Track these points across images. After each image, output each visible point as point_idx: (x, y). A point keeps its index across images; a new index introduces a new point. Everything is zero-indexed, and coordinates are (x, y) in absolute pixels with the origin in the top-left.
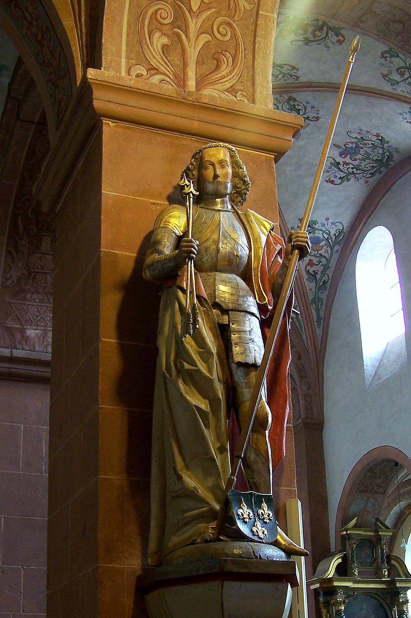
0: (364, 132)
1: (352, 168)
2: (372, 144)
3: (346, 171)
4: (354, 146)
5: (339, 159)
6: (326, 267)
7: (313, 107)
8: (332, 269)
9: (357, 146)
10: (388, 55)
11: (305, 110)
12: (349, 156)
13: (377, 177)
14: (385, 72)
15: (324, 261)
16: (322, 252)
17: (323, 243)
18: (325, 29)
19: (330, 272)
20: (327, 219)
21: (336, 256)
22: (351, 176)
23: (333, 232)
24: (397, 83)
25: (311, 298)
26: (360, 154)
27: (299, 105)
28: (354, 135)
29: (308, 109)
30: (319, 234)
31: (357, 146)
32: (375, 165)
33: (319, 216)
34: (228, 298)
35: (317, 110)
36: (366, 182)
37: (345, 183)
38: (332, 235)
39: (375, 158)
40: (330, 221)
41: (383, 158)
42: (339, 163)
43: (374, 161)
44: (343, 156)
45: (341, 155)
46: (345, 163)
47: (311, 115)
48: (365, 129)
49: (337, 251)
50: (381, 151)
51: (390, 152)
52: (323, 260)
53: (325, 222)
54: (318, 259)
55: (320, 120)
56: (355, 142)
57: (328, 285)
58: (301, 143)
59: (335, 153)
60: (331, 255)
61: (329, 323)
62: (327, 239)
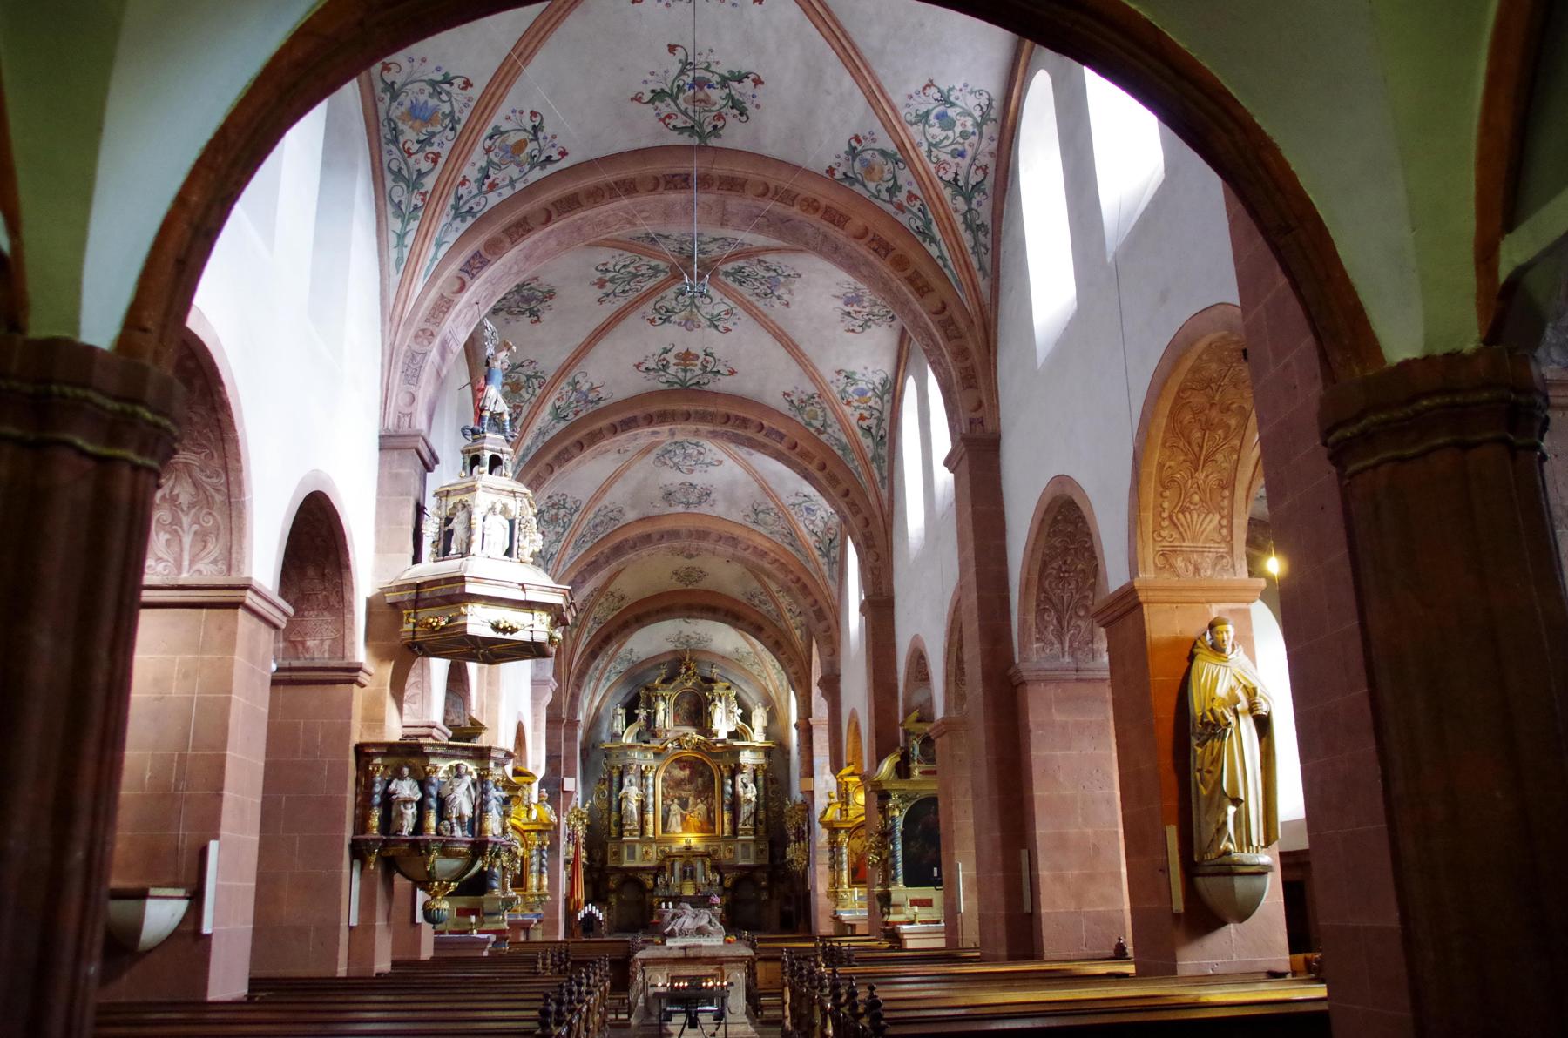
5: (848, 309)
6: (880, 420)
8: (888, 420)
15: (876, 414)
16: (871, 403)
17: (870, 394)
19: (886, 425)
20: (866, 368)
21: (888, 407)
23: (877, 380)
25: (870, 455)
29: (784, 268)
30: (862, 385)
33: (855, 366)
36: (890, 326)
37: (867, 330)
38: (877, 384)
40: (870, 370)
42: (849, 313)
45: (846, 304)
46: (856, 312)
49: (888, 401)
52: (875, 412)
53: (865, 372)
54: (868, 412)
55: (803, 276)
57: (886, 439)
58: (798, 298)
59: (840, 304)
60: (883, 408)
61: (892, 483)
62: (873, 390)
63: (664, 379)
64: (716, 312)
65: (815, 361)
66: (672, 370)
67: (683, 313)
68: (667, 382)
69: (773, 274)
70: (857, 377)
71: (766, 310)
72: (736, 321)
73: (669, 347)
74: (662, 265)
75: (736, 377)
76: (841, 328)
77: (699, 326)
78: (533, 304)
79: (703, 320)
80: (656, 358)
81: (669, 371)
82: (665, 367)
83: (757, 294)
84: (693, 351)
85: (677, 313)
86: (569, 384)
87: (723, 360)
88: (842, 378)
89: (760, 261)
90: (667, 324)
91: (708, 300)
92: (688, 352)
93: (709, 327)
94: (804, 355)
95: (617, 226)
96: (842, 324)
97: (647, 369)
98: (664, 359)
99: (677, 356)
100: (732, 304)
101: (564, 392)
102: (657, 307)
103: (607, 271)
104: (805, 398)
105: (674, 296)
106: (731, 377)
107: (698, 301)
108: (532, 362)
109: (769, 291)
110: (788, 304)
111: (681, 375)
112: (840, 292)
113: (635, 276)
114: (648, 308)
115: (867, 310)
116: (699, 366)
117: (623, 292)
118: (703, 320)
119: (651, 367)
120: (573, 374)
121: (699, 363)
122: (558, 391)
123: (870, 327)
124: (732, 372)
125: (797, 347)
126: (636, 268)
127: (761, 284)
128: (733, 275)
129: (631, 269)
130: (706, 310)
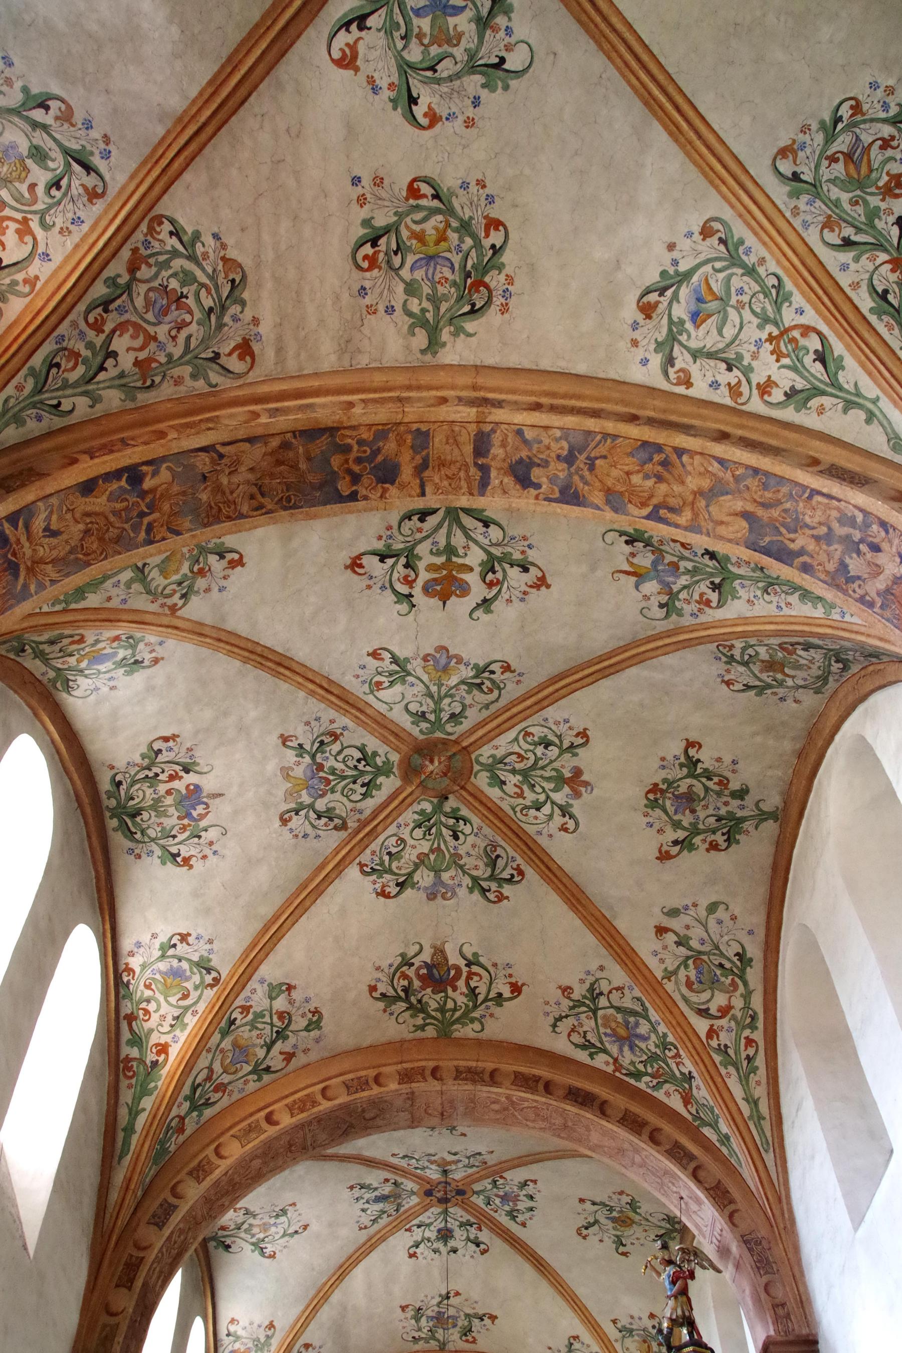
0: (208, 851)
1: (157, 775)
2: (174, 837)
3: (162, 766)
4: (195, 814)
5: (191, 778)
7: (305, 836)
9: (188, 815)
10: (315, 1019)
11: (311, 823)
12: (184, 792)
13: (105, 785)
14: (294, 994)
18: (402, 994)
22: (146, 762)
24: (272, 998)
26: (170, 806)
27: (326, 825)
28: (212, 834)
29: (309, 830)
31: (188, 815)
32: (131, 803)
34: (172, 435)
35: (297, 836)
36: (112, 767)
37: (144, 749)
39: (145, 815)
40: (105, 689)
41: (135, 824)
43: (142, 809)
44: (192, 787)
47: (296, 822)
48: (212, 859)
50: (152, 833)
51: (138, 841)
55: (278, 823)
56: (200, 820)
58: (272, 766)
59: (208, 784)
63: (495, 533)
64: (398, 688)
65: (205, 652)
66: (475, 557)
67: (454, 680)
68: (486, 525)
69: (321, 805)
70: (122, 671)
71: (315, 707)
72: (361, 672)
73: (479, 613)
74: (482, 780)
75: (345, 557)
76: (186, 730)
77: (425, 659)
78: (683, 789)
79: (420, 672)
80: (505, 595)
81: (480, 556)
82: (489, 567)
83: (336, 737)
84: (435, 602)
85: (463, 682)
86: (680, 613)
87: (376, 589)
88: (148, 657)
89: (344, 826)
90: (482, 664)
91: (413, 707)
92: (444, 598)
93: (407, 660)
94: (230, 653)
95: (526, 1104)
96: (188, 745)
97: (526, 570)
98: (491, 585)
99: (464, 590)
100: (370, 699)
101: (694, 607)
102: (496, 692)
103: (565, 811)
104: (201, 583)
105: (468, 713)
106: (354, 555)
107: (428, 705)
108: (728, 683)
109: (319, 758)
110: (284, 740)
111: (458, 539)
112: (220, 811)
113: (525, 774)
114: (512, 691)
115: (162, 788)
116: (421, 565)
117: (547, 744)
118: (420, 672)
119: (516, 569)
120: (662, 626)
121: (424, 576)
122: (703, 619)
123: (143, 756)
124: (355, 565)
125: (246, 660)
126: (521, 795)
127: (333, 771)
128: (380, 771)
129: (530, 797)
130: (415, 690)
